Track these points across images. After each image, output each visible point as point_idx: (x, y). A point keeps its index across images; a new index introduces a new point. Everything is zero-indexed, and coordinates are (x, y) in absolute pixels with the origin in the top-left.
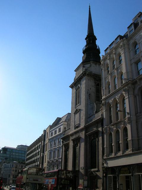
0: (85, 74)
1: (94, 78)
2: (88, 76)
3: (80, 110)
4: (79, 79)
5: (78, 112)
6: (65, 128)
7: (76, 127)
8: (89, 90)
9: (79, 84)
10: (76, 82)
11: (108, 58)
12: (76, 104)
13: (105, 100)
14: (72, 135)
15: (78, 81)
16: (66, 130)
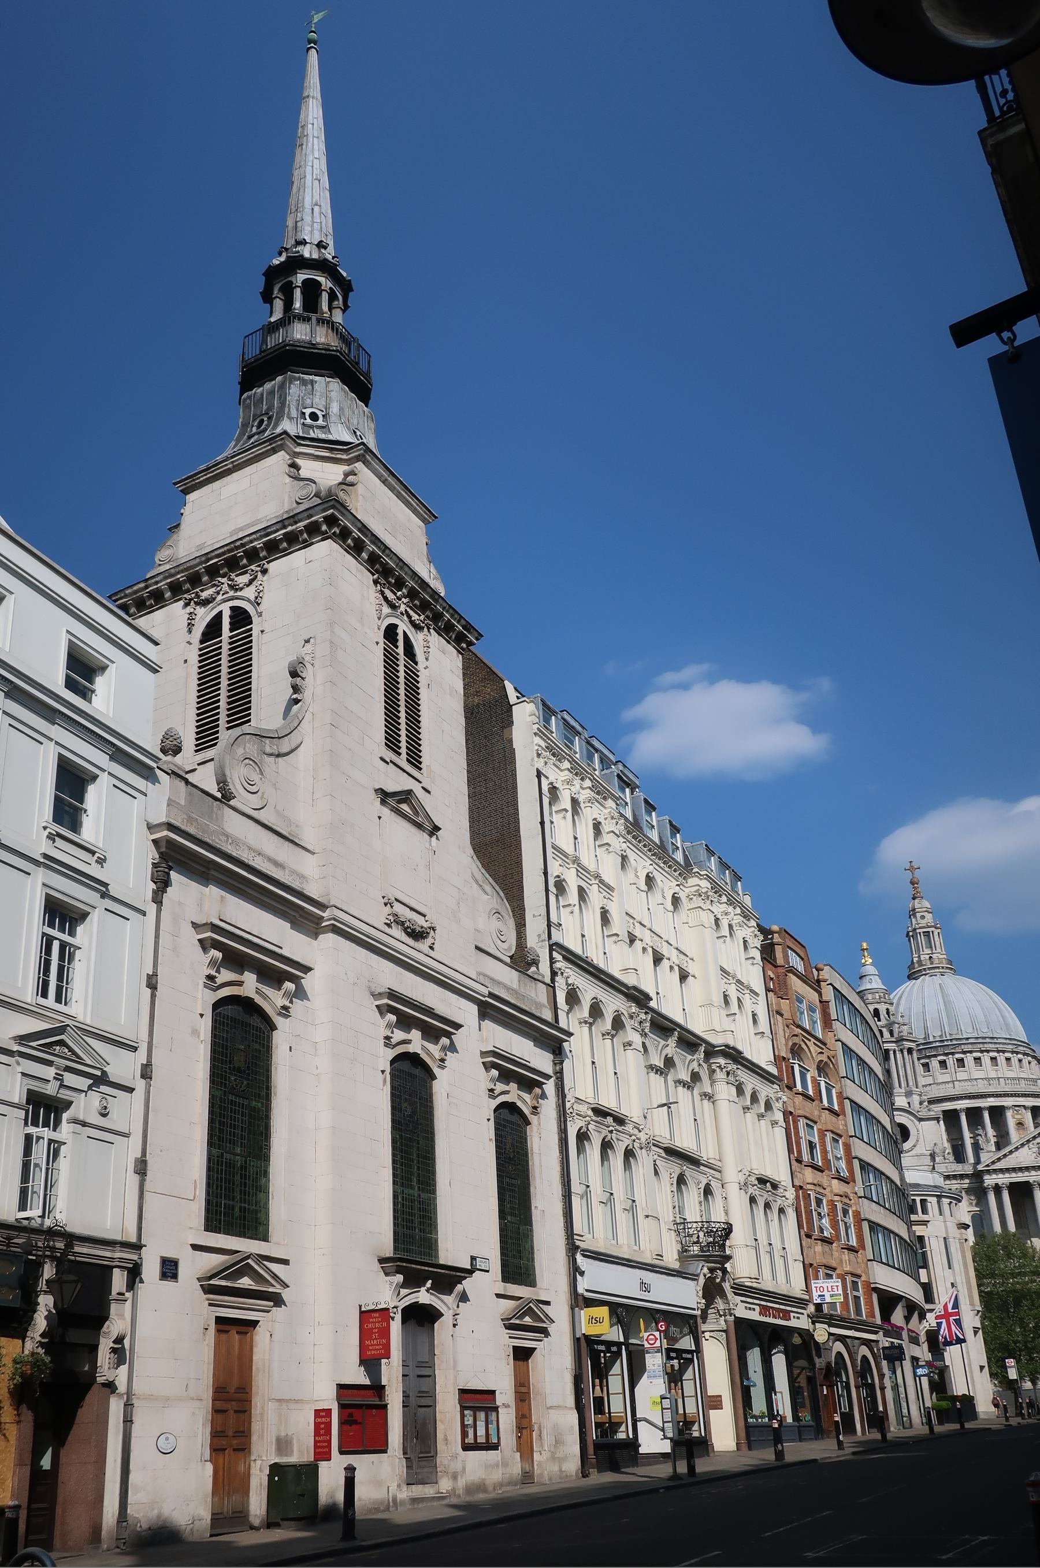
5: (419, 826)
9: (417, 627)
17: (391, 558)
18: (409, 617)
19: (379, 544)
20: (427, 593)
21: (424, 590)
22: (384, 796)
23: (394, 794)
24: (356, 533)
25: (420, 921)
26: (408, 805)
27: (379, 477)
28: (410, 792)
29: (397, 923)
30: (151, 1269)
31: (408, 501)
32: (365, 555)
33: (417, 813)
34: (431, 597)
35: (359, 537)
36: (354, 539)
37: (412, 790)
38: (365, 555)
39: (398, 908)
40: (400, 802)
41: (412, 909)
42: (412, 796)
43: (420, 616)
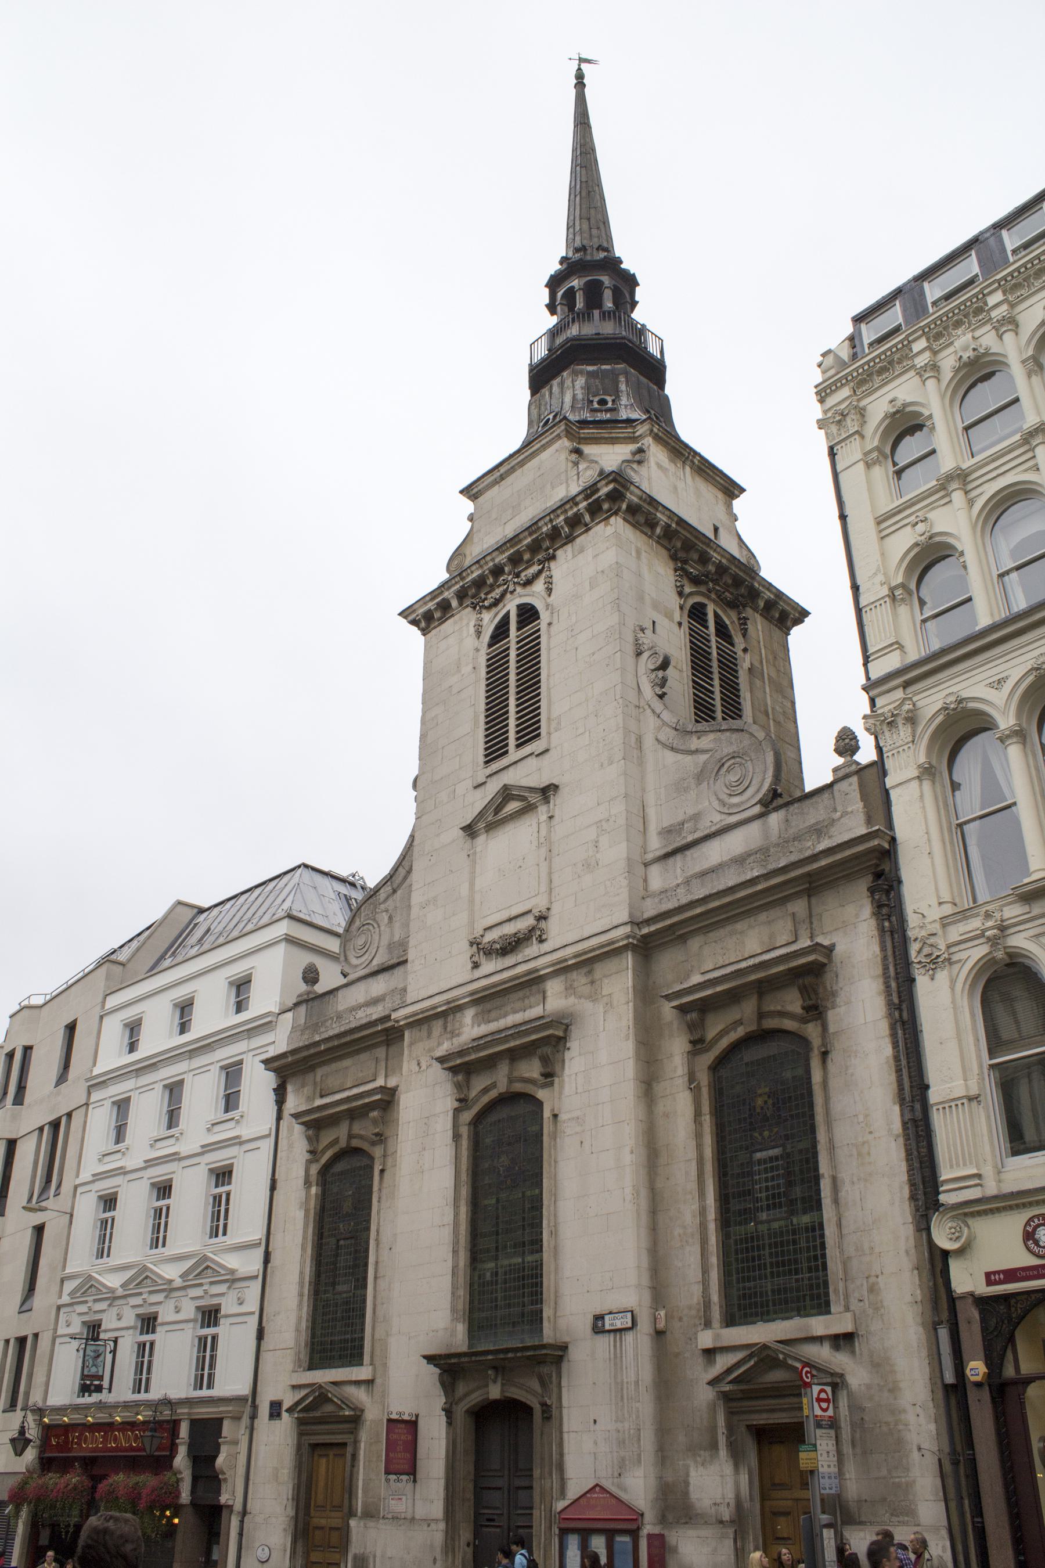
0: (615, 496)
1: (674, 558)
2: (635, 525)
3: (548, 791)
4: (535, 548)
5: (529, 808)
6: (311, 976)
7: (510, 946)
8: (643, 630)
9: (529, 582)
10: (497, 571)
11: (921, 361)
12: (495, 750)
13: (906, 685)
14: (448, 1013)
15: (516, 560)
16: (320, 988)
17: (472, 572)
18: (519, 583)
19: (453, 582)
20: (525, 538)
21: (520, 541)
22: (470, 830)
23: (481, 814)
24: (431, 605)
25: (529, 921)
26: (513, 799)
27: (496, 482)
28: (506, 787)
29: (490, 953)
30: (264, 1410)
31: (531, 454)
32: (454, 603)
33: (522, 798)
34: (530, 534)
35: (438, 604)
36: (436, 609)
37: (505, 785)
38: (454, 603)
39: (490, 937)
40: (497, 811)
41: (510, 920)
42: (509, 789)
43: (534, 563)
